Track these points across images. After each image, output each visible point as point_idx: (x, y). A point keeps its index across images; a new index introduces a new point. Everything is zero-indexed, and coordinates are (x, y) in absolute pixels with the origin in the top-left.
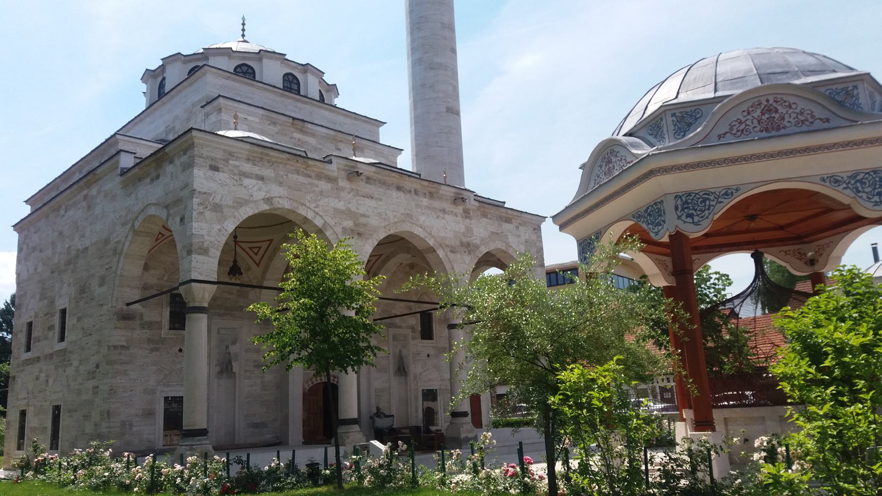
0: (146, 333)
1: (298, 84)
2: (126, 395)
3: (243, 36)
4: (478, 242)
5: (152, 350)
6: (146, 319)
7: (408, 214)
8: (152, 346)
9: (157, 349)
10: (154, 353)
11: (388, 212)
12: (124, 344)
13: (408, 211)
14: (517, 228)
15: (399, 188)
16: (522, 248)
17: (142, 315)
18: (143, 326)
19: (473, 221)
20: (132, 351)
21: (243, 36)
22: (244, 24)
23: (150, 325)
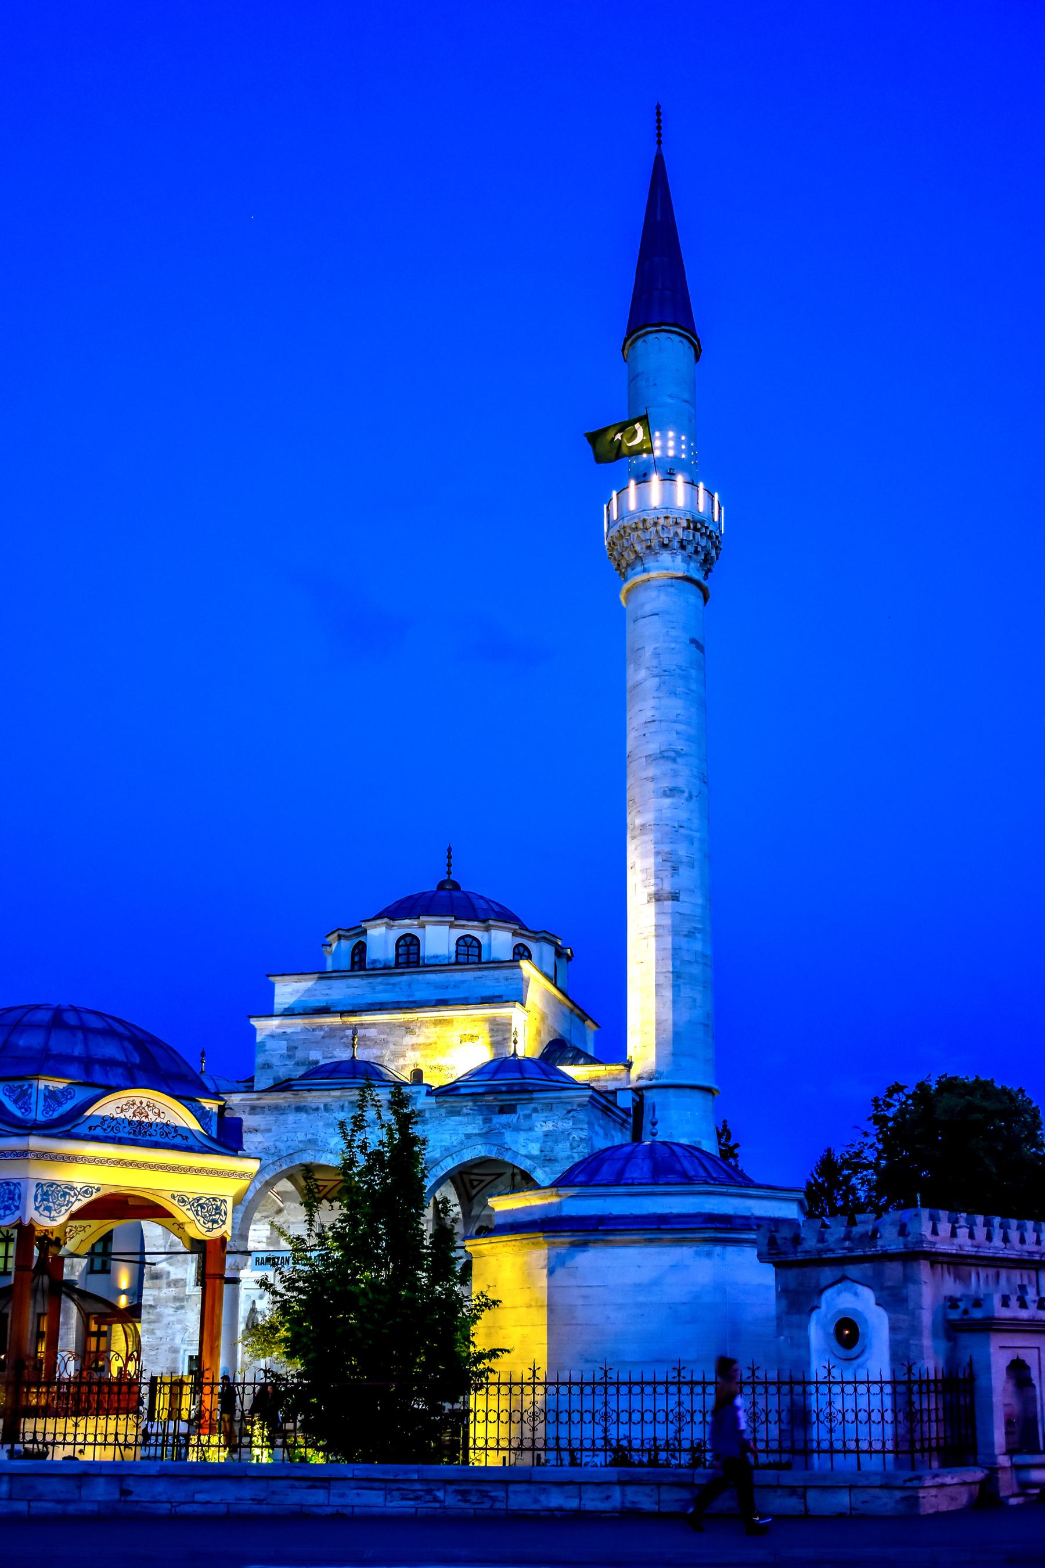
0: (172, 1292)
1: (418, 945)
2: (153, 1353)
3: (449, 873)
4: (437, 1154)
5: (178, 1308)
6: (173, 1277)
7: (309, 1140)
8: (178, 1304)
9: (182, 1307)
10: (179, 1312)
11: (278, 1143)
12: (151, 1303)
13: (310, 1137)
14: (528, 1117)
15: (299, 1109)
16: (535, 1149)
17: (169, 1273)
18: (169, 1285)
19: (429, 1126)
20: (158, 1310)
21: (449, 873)
22: (449, 857)
23: (176, 1283)
